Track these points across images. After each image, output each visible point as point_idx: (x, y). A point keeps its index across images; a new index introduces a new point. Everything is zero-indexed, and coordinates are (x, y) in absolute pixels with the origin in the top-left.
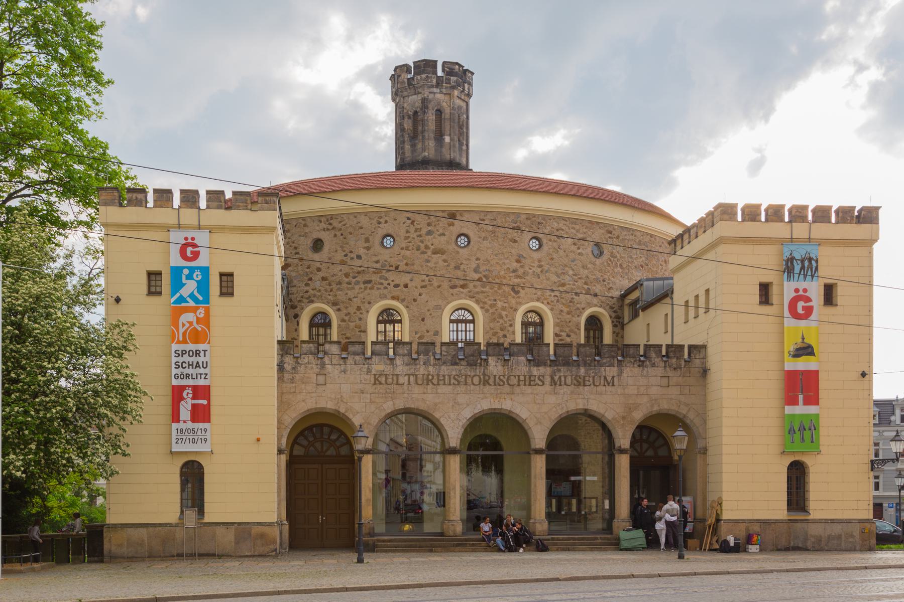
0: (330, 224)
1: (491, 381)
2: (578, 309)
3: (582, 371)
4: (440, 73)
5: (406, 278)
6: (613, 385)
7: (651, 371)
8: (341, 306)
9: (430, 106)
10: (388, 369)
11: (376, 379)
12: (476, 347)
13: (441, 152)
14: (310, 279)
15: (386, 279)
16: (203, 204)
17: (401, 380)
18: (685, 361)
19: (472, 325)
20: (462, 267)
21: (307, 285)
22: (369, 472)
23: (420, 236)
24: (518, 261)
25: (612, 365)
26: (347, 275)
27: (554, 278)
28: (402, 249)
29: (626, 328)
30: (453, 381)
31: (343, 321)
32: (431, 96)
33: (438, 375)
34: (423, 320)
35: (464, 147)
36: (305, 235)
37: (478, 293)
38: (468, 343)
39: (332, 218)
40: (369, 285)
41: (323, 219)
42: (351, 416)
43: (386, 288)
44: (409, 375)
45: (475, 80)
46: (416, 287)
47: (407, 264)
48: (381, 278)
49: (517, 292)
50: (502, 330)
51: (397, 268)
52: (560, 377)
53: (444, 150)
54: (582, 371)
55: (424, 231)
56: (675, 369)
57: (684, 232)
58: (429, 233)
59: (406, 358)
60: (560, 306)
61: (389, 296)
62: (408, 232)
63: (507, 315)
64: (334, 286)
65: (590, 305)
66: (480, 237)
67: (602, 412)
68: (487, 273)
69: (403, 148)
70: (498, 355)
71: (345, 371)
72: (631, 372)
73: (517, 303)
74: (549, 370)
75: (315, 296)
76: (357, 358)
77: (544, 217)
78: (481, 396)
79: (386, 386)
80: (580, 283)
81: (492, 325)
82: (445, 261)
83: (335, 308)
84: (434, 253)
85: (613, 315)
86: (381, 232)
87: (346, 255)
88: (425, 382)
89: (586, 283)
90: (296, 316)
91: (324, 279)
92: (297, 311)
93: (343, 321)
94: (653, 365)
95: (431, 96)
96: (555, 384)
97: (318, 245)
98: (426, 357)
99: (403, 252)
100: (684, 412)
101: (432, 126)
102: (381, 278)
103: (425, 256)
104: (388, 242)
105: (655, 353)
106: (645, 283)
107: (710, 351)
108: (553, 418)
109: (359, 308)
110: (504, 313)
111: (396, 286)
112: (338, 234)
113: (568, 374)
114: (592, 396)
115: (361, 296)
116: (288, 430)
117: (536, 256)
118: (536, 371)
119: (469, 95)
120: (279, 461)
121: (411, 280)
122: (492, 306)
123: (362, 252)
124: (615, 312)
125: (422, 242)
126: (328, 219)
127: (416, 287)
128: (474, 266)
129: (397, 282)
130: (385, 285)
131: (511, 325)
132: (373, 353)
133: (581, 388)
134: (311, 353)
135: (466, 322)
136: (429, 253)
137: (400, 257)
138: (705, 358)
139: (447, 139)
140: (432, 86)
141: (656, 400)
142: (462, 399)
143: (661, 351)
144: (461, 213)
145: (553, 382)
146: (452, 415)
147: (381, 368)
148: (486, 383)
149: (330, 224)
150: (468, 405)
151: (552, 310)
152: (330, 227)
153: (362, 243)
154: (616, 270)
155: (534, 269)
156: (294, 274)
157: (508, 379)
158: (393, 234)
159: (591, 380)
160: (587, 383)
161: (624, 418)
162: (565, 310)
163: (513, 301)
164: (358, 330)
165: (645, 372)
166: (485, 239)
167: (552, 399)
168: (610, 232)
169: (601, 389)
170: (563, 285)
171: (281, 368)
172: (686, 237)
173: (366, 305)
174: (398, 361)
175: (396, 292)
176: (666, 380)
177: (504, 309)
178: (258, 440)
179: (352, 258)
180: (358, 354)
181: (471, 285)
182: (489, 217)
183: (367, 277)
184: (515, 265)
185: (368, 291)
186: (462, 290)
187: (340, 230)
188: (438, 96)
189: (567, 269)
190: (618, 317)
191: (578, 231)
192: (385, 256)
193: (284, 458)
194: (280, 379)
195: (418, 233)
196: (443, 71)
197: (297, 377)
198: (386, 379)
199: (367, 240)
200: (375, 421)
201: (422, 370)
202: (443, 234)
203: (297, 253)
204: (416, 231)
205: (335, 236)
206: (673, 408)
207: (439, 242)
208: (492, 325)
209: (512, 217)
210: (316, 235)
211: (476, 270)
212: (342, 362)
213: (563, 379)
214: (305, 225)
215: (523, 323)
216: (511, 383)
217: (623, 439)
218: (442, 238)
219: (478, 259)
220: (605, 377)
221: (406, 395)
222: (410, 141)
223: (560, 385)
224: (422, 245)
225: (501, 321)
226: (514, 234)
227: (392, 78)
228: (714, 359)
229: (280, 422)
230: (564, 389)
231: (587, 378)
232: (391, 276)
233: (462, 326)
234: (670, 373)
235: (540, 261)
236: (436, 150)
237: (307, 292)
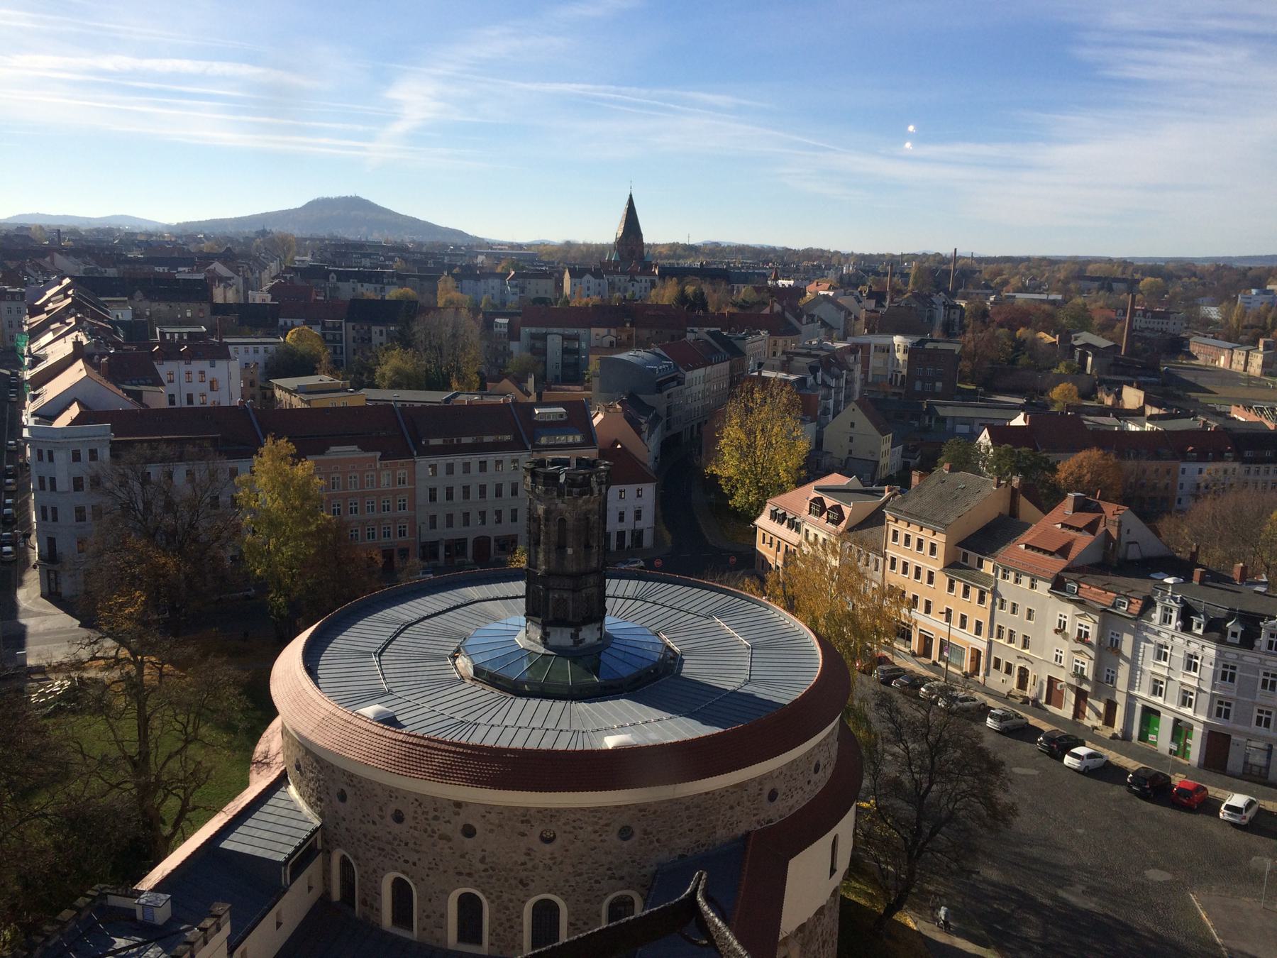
5: (414, 857)
50: (508, 920)
51: (406, 844)
55: (430, 816)
58: (436, 818)
77: (558, 810)
84: (442, 837)
89: (609, 869)
109: (375, 871)
111: (406, 862)
122: (499, 897)
123: (377, 819)
128: (479, 855)
136: (436, 836)
144: (467, 804)
151: (566, 900)
166: (491, 831)
170: (581, 874)
199: (381, 809)
211: (483, 860)
226: (523, 828)
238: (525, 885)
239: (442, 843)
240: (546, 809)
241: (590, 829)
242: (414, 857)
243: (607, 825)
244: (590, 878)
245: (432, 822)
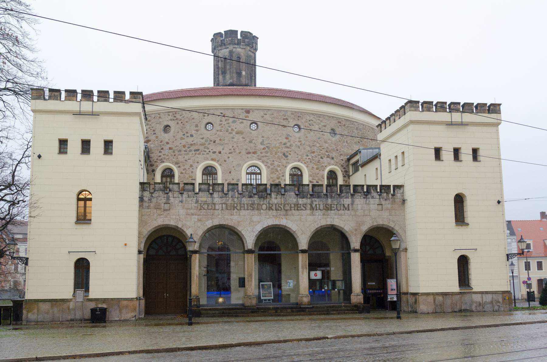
0: (175, 117)
1: (274, 207)
2: (323, 166)
3: (329, 201)
4: (239, 37)
6: (349, 210)
7: (372, 201)
8: (181, 165)
10: (209, 200)
11: (201, 206)
12: (264, 187)
13: (240, 80)
14: (162, 149)
15: (208, 149)
16: (95, 99)
17: (217, 207)
18: (392, 195)
19: (260, 176)
20: (253, 141)
21: (160, 152)
22: (197, 266)
23: (228, 123)
24: (287, 138)
25: (347, 198)
26: (184, 146)
27: (308, 148)
28: (218, 131)
29: (351, 178)
30: (249, 208)
31: (182, 173)
32: (234, 50)
33: (240, 204)
34: (230, 172)
35: (253, 78)
36: (160, 123)
37: (263, 157)
38: (258, 185)
39: (176, 113)
40: (198, 152)
41: (170, 114)
42: (185, 230)
43: (207, 154)
44: (222, 204)
45: (259, 41)
46: (226, 153)
47: (220, 140)
48: (205, 148)
50: (278, 178)
51: (214, 142)
52: (316, 205)
54: (329, 201)
56: (386, 200)
57: (382, 123)
59: (220, 193)
60: (312, 165)
61: (210, 159)
62: (221, 121)
63: (280, 170)
64: (176, 152)
65: (330, 164)
67: (342, 226)
68: (268, 145)
69: (218, 78)
70: (279, 192)
71: (182, 202)
72: (359, 201)
73: (287, 163)
74: (309, 201)
75: (165, 158)
76: (190, 193)
78: (268, 217)
79: (208, 211)
80: (323, 151)
81: (272, 176)
82: (243, 138)
83: (177, 166)
84: (237, 133)
85: (343, 170)
86: (205, 121)
87: (184, 135)
88: (232, 208)
89: (327, 152)
90: (153, 171)
91: (170, 149)
92: (154, 167)
93: (182, 173)
94: (373, 197)
95: (234, 50)
96: (313, 209)
97: (167, 128)
98: (233, 193)
99: (218, 133)
100: (392, 226)
102: (205, 148)
103: (231, 135)
104: (209, 127)
105: (374, 190)
106: (362, 151)
107: (406, 188)
108: (312, 230)
109: (191, 166)
110: (279, 169)
111: (214, 152)
112: (180, 122)
113: (321, 203)
114: (336, 217)
115: (193, 158)
116: (145, 239)
117: (298, 135)
118: (301, 201)
119: (256, 50)
120: (139, 258)
122: (272, 164)
123: (193, 132)
124: (344, 168)
125: (229, 127)
126: (174, 112)
127: (226, 153)
128: (260, 141)
129: (214, 150)
130: (207, 152)
131: (283, 176)
132: (200, 190)
133: (329, 211)
134: (161, 190)
135: (256, 174)
136: (234, 133)
137: (216, 136)
138: (403, 193)
139: (244, 73)
140: (235, 44)
141: (375, 219)
142: (255, 219)
143: (377, 190)
144: (253, 110)
145: (312, 208)
146: (249, 229)
147: (204, 199)
148: (270, 209)
149: (175, 117)
150: (259, 222)
151: (307, 167)
152: (175, 118)
153: (193, 128)
154: (344, 144)
155: (296, 143)
156: (152, 146)
157: (284, 206)
158: (212, 122)
159: (335, 206)
160: (333, 209)
161: (356, 230)
162: (315, 167)
163: (284, 162)
164: (190, 179)
165: (368, 202)
167: (311, 218)
168: (340, 122)
169: (342, 212)
170: (313, 152)
171: (141, 199)
172: (383, 126)
173: (196, 164)
174: (215, 195)
175: (214, 156)
176: (380, 206)
177: (279, 166)
178: (126, 245)
179: (188, 137)
180: (190, 191)
181: (259, 153)
182: (270, 112)
183: (196, 148)
184: (285, 141)
185: (197, 155)
187: (181, 120)
188: (239, 50)
189: (315, 143)
190: (346, 172)
191: (321, 121)
192: (207, 134)
193: (142, 256)
194: (141, 206)
195: (227, 122)
196: (241, 36)
197: (152, 205)
198: (208, 206)
199: (197, 126)
200: (200, 232)
201: (230, 201)
203: (155, 134)
205: (178, 123)
206: (385, 223)
208: (272, 176)
209: (283, 113)
210: (166, 123)
212: (180, 195)
213: (318, 206)
214: (160, 117)
215: (290, 175)
216: (286, 209)
217: (355, 242)
219: (263, 137)
220: (344, 205)
221: (220, 216)
222: (222, 74)
223: (316, 210)
224: (230, 129)
225: (277, 173)
227: (212, 40)
228: (409, 193)
229: (140, 233)
230: (318, 213)
231: (333, 206)
232: (212, 147)
233: (253, 176)
234: (383, 202)
235: (299, 138)
236: (237, 79)
237: (160, 156)
238: (286, 156)
239: (237, 136)
240: (296, 112)
242: (220, 148)
243: (325, 126)
244: (319, 155)
245: (233, 124)
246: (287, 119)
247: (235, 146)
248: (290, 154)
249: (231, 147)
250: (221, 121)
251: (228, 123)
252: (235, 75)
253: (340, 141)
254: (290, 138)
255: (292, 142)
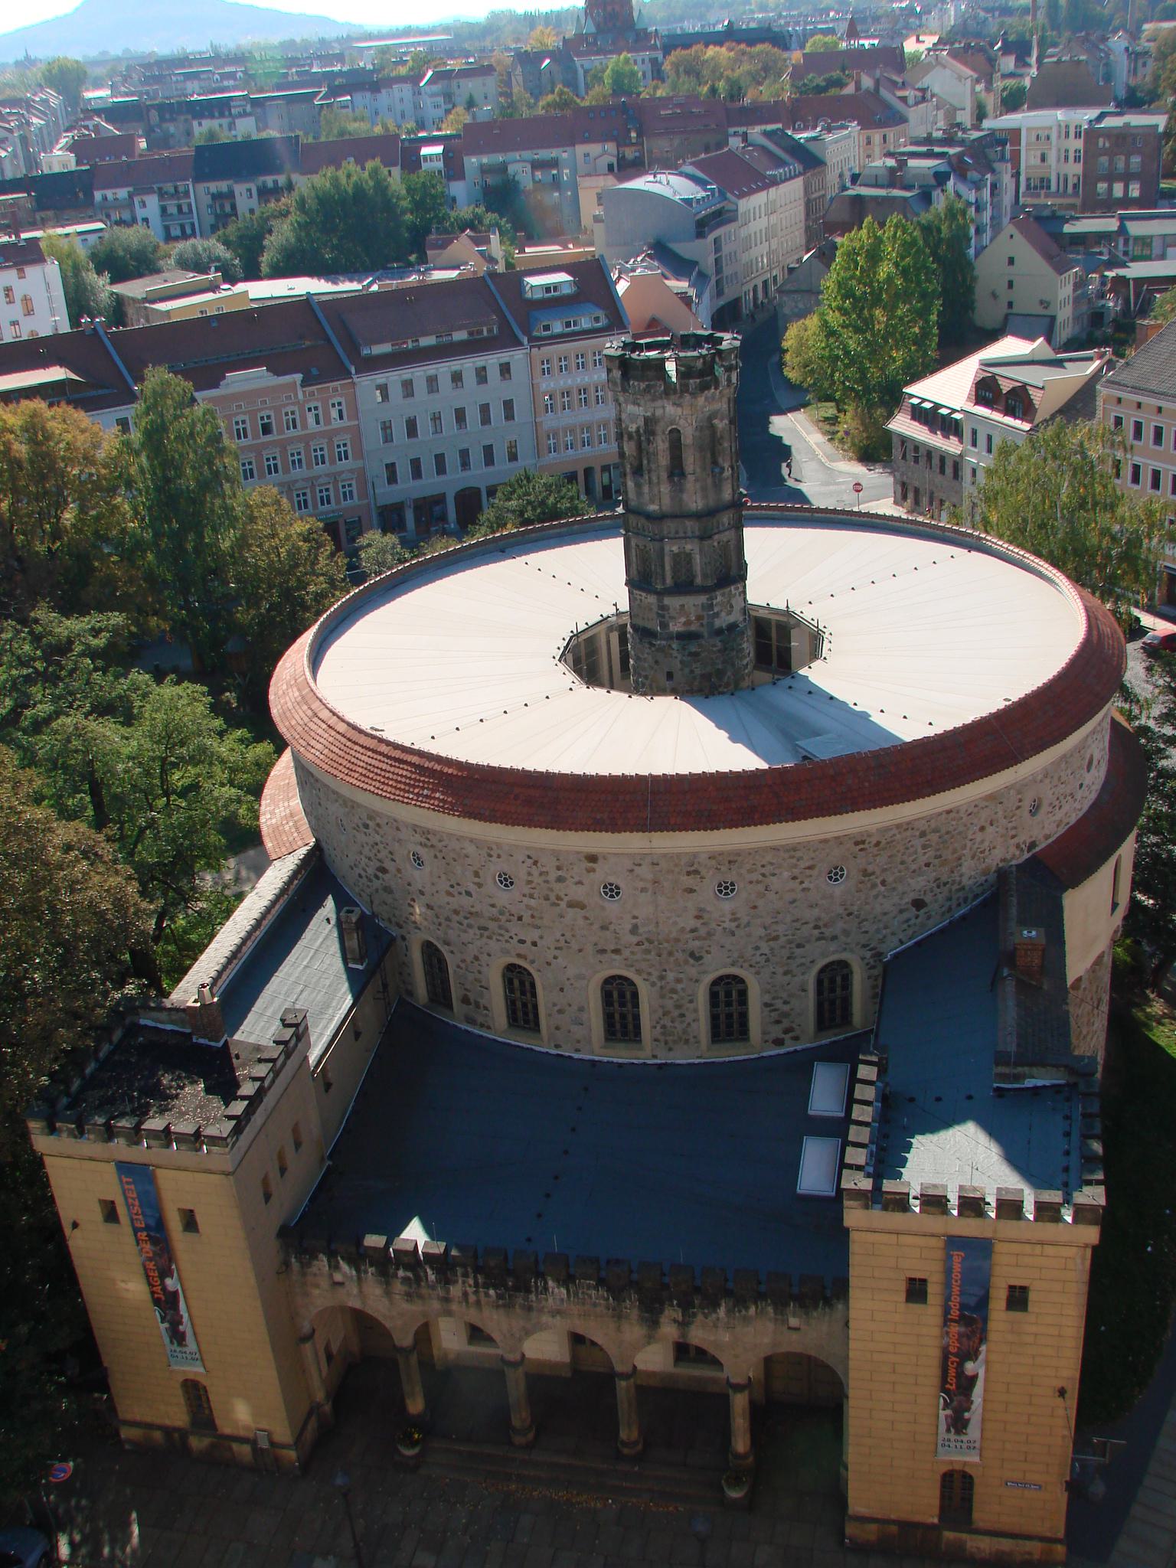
9: (659, 429)
13: (681, 500)
20: (612, 927)
23: (547, 882)
24: (698, 917)
27: (762, 932)
40: (486, 934)
48: (500, 927)
49: (700, 958)
51: (520, 918)
53: (685, 497)
55: (552, 877)
58: (560, 879)
62: (529, 874)
66: (636, 889)
82: (586, 918)
84: (570, 905)
89: (816, 927)
95: (659, 413)
99: (526, 900)
101: (664, 460)
103: (557, 910)
110: (679, 987)
115: (478, 943)
121: (541, 937)
122: (662, 978)
123: (472, 888)
131: (691, 1001)
136: (563, 904)
162: (780, 970)
163: (692, 971)
166: (643, 890)
170: (776, 938)
181: (626, 953)
183: (482, 922)
185: (484, 940)
186: (614, 956)
195: (543, 878)
199: (477, 874)
202: (580, 883)
204: (541, 874)
207: (577, 893)
211: (634, 930)
218: (580, 888)
219: (635, 917)
224: (553, 898)
232: (515, 928)
236: (672, 499)
241: (786, 874)
243: (809, 868)
244: (790, 942)
246: (696, 872)
247: (568, 935)
248: (708, 952)
249: (558, 935)
250: (529, 874)
251: (547, 882)
252: (665, 489)
253: (859, 891)
254: (706, 916)
255: (713, 925)
